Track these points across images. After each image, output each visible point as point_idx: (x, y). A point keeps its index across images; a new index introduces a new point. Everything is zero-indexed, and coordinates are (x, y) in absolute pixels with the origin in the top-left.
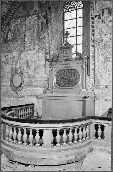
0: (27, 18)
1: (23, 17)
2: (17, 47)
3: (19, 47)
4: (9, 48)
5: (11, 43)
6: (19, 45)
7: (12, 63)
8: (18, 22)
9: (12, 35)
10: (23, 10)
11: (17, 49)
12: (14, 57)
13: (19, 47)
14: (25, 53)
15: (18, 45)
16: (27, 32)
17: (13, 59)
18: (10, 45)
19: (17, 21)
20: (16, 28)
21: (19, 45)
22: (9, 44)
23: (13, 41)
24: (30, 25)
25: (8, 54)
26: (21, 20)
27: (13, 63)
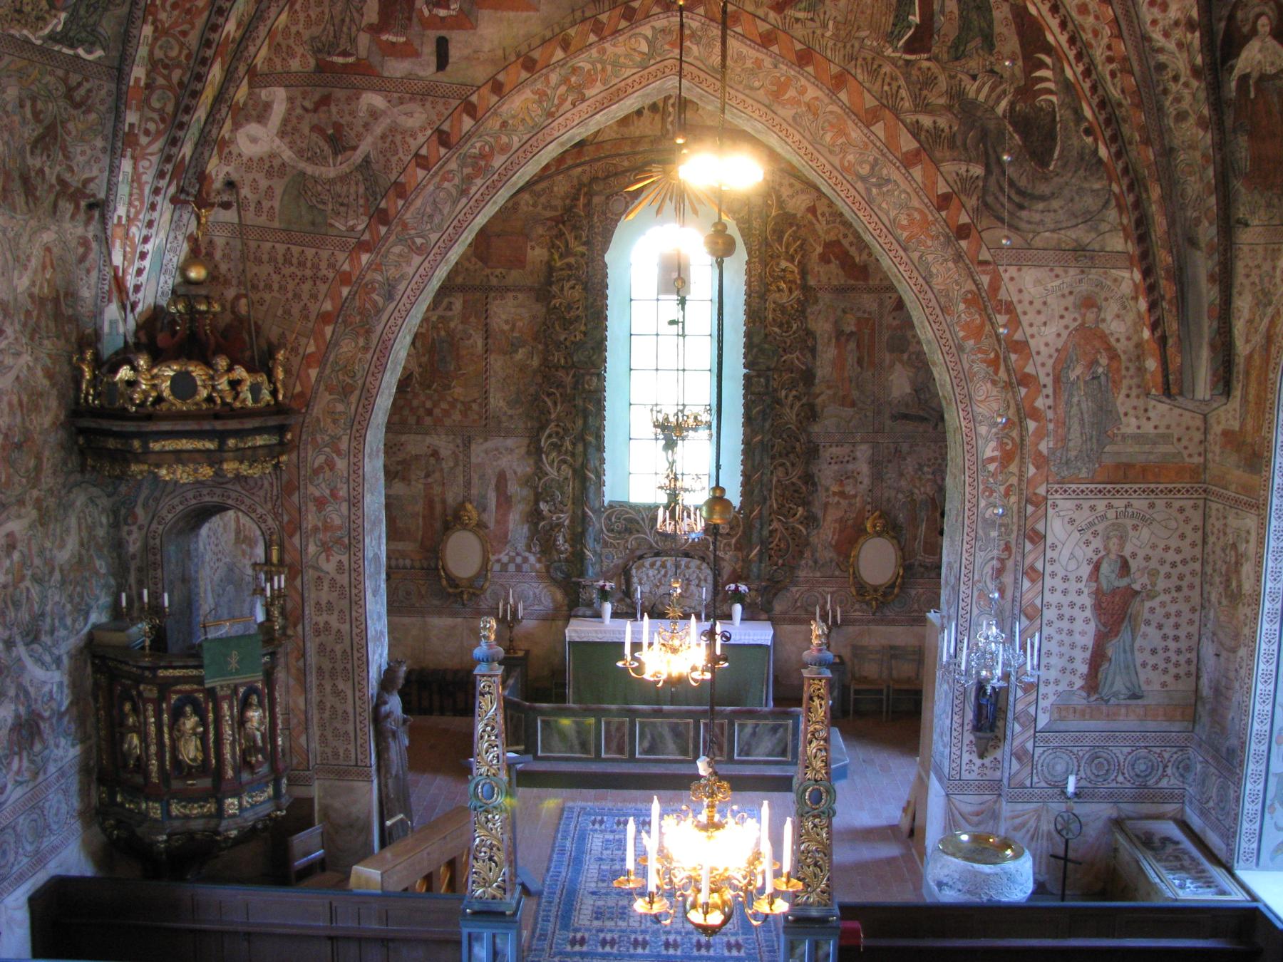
0: (495, 298)
1: (475, 289)
2: (447, 413)
3: (457, 416)
4: (406, 412)
5: (416, 395)
6: (459, 405)
7: (427, 476)
8: (449, 308)
9: (424, 359)
10: (474, 259)
11: (448, 422)
12: (435, 454)
13: (457, 416)
14: (489, 444)
15: (453, 405)
16: (492, 358)
17: (432, 460)
18: (415, 403)
19: (446, 301)
20: (443, 333)
21: (459, 405)
22: (409, 396)
23: (429, 387)
24: (512, 330)
25: (404, 438)
26: (465, 302)
27: (430, 480)
